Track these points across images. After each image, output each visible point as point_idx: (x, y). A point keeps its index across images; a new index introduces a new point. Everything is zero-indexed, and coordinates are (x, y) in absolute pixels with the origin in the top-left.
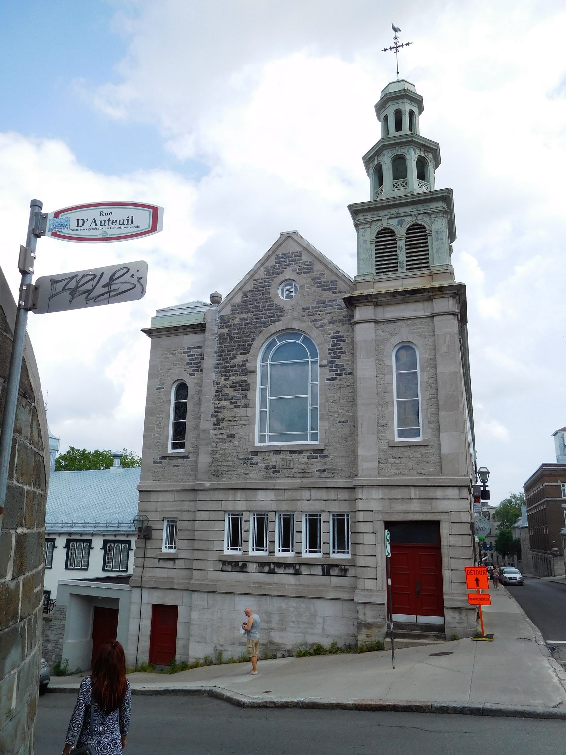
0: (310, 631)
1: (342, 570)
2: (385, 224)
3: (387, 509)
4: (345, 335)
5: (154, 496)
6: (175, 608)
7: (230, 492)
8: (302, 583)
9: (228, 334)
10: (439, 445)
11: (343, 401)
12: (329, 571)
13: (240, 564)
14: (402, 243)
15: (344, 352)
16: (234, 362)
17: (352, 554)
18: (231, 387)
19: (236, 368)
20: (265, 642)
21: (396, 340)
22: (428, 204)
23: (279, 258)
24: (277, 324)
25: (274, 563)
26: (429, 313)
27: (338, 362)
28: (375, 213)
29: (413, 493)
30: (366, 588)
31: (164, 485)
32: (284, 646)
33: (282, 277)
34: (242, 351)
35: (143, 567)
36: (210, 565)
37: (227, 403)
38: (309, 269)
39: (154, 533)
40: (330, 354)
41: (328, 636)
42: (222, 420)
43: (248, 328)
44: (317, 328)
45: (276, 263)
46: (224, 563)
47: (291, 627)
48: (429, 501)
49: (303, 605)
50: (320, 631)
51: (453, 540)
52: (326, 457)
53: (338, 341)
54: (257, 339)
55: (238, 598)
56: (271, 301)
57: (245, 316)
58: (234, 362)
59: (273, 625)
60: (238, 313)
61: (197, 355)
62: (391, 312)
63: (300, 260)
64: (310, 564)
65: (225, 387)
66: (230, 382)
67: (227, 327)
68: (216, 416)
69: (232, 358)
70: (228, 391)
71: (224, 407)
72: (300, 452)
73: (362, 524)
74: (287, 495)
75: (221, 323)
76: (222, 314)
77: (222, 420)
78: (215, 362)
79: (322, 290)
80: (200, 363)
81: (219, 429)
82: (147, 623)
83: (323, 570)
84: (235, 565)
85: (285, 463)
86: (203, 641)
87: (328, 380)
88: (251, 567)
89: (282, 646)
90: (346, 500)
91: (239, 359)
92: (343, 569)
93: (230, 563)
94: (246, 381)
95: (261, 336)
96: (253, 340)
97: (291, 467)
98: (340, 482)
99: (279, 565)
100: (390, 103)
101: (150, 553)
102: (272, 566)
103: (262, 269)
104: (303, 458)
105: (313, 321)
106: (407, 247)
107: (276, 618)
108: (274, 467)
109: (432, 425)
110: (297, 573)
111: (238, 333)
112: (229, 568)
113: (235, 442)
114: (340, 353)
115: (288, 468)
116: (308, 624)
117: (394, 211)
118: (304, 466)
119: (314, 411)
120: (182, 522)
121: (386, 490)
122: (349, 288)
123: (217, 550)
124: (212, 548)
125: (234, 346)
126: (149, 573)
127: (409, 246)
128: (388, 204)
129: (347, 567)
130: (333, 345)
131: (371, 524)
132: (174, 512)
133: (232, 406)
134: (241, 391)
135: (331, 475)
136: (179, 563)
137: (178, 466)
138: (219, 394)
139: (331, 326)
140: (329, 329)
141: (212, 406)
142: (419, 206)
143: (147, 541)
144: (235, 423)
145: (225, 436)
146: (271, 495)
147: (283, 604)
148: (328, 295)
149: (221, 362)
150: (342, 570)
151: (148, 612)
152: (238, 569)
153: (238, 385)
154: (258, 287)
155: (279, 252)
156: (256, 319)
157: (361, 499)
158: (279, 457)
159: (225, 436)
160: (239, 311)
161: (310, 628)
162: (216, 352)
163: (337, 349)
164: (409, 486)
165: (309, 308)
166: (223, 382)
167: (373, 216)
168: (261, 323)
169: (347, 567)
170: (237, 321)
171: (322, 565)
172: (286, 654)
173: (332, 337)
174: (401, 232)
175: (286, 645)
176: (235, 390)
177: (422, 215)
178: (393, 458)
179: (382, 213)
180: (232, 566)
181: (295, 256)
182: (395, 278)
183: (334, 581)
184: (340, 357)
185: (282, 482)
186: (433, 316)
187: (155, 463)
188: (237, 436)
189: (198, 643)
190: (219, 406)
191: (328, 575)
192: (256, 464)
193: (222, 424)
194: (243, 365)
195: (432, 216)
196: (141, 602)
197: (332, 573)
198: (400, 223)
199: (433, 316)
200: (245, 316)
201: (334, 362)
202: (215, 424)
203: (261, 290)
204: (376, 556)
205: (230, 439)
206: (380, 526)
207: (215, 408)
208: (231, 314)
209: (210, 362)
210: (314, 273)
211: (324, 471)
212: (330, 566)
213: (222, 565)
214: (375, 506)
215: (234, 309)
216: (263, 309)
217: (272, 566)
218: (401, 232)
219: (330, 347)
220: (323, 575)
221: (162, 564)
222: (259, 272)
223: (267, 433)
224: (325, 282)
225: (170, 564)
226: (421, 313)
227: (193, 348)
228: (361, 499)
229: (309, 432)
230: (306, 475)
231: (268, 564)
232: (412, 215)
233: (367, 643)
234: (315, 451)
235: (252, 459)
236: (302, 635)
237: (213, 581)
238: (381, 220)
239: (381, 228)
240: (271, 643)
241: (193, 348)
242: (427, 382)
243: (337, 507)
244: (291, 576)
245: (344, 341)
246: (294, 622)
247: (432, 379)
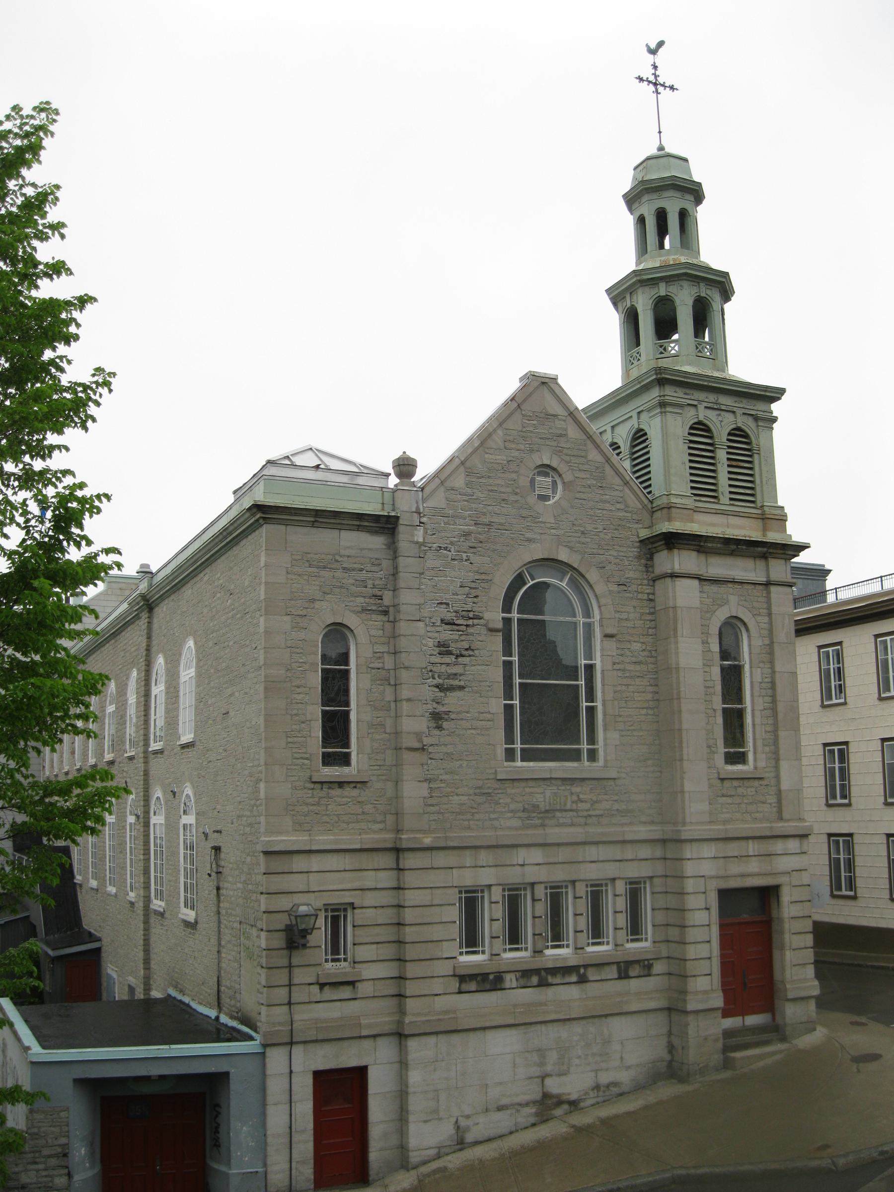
1: (644, 966)
2: (703, 414)
5: (299, 863)
6: (361, 1072)
7: (468, 852)
10: (778, 777)
11: (639, 699)
12: (626, 971)
13: (491, 977)
14: (722, 455)
17: (654, 942)
21: (722, 614)
22: (754, 402)
24: (533, 546)
26: (763, 579)
28: (688, 391)
29: (752, 847)
30: (699, 989)
31: (323, 840)
32: (568, 1097)
35: (290, 1004)
36: (437, 986)
41: (628, 1068)
46: (462, 979)
47: (576, 1065)
48: (767, 858)
49: (592, 1029)
55: (490, 1034)
59: (549, 1068)
62: (719, 567)
64: (600, 966)
73: (691, 897)
74: (563, 854)
82: (305, 1108)
85: (558, 800)
86: (434, 1115)
88: (510, 980)
89: (565, 1098)
90: (646, 859)
92: (646, 966)
93: (472, 977)
98: (643, 831)
99: (553, 971)
100: (670, 193)
101: (301, 976)
102: (543, 973)
106: (729, 463)
107: (552, 1056)
109: (767, 749)
110: (583, 980)
112: (473, 986)
115: (563, 808)
116: (601, 1055)
117: (712, 397)
119: (591, 711)
120: (364, 910)
121: (721, 845)
122: (641, 507)
123: (447, 958)
124: (439, 955)
126: (301, 1015)
127: (731, 461)
128: (710, 384)
129: (651, 962)
131: (703, 895)
132: (347, 893)
136: (365, 989)
142: (744, 401)
143: (294, 953)
146: (537, 856)
147: (562, 1032)
150: (644, 966)
151: (304, 1088)
152: (488, 987)
157: (689, 859)
161: (603, 1061)
164: (747, 838)
167: (688, 397)
169: (651, 962)
171: (618, 963)
174: (721, 435)
175: (569, 1094)
177: (746, 417)
178: (723, 796)
179: (701, 395)
180: (478, 982)
182: (718, 512)
183: (634, 984)
185: (555, 833)
186: (768, 584)
189: (425, 1122)
191: (627, 977)
195: (760, 424)
196: (291, 1072)
197: (631, 973)
199: (768, 584)
204: (709, 942)
206: (713, 900)
212: (629, 964)
213: (461, 982)
214: (708, 869)
217: (543, 973)
218: (721, 435)
220: (620, 978)
221: (328, 993)
222: (494, 437)
223: (518, 746)
225: (346, 992)
226: (752, 576)
228: (689, 859)
229: (585, 746)
231: (537, 971)
232: (734, 412)
233: (701, 1065)
236: (593, 1074)
237: (446, 1012)
238: (695, 406)
239: (696, 420)
240: (546, 1096)
242: (761, 683)
243: (634, 871)
244: (573, 986)
246: (579, 1057)
247: (766, 680)
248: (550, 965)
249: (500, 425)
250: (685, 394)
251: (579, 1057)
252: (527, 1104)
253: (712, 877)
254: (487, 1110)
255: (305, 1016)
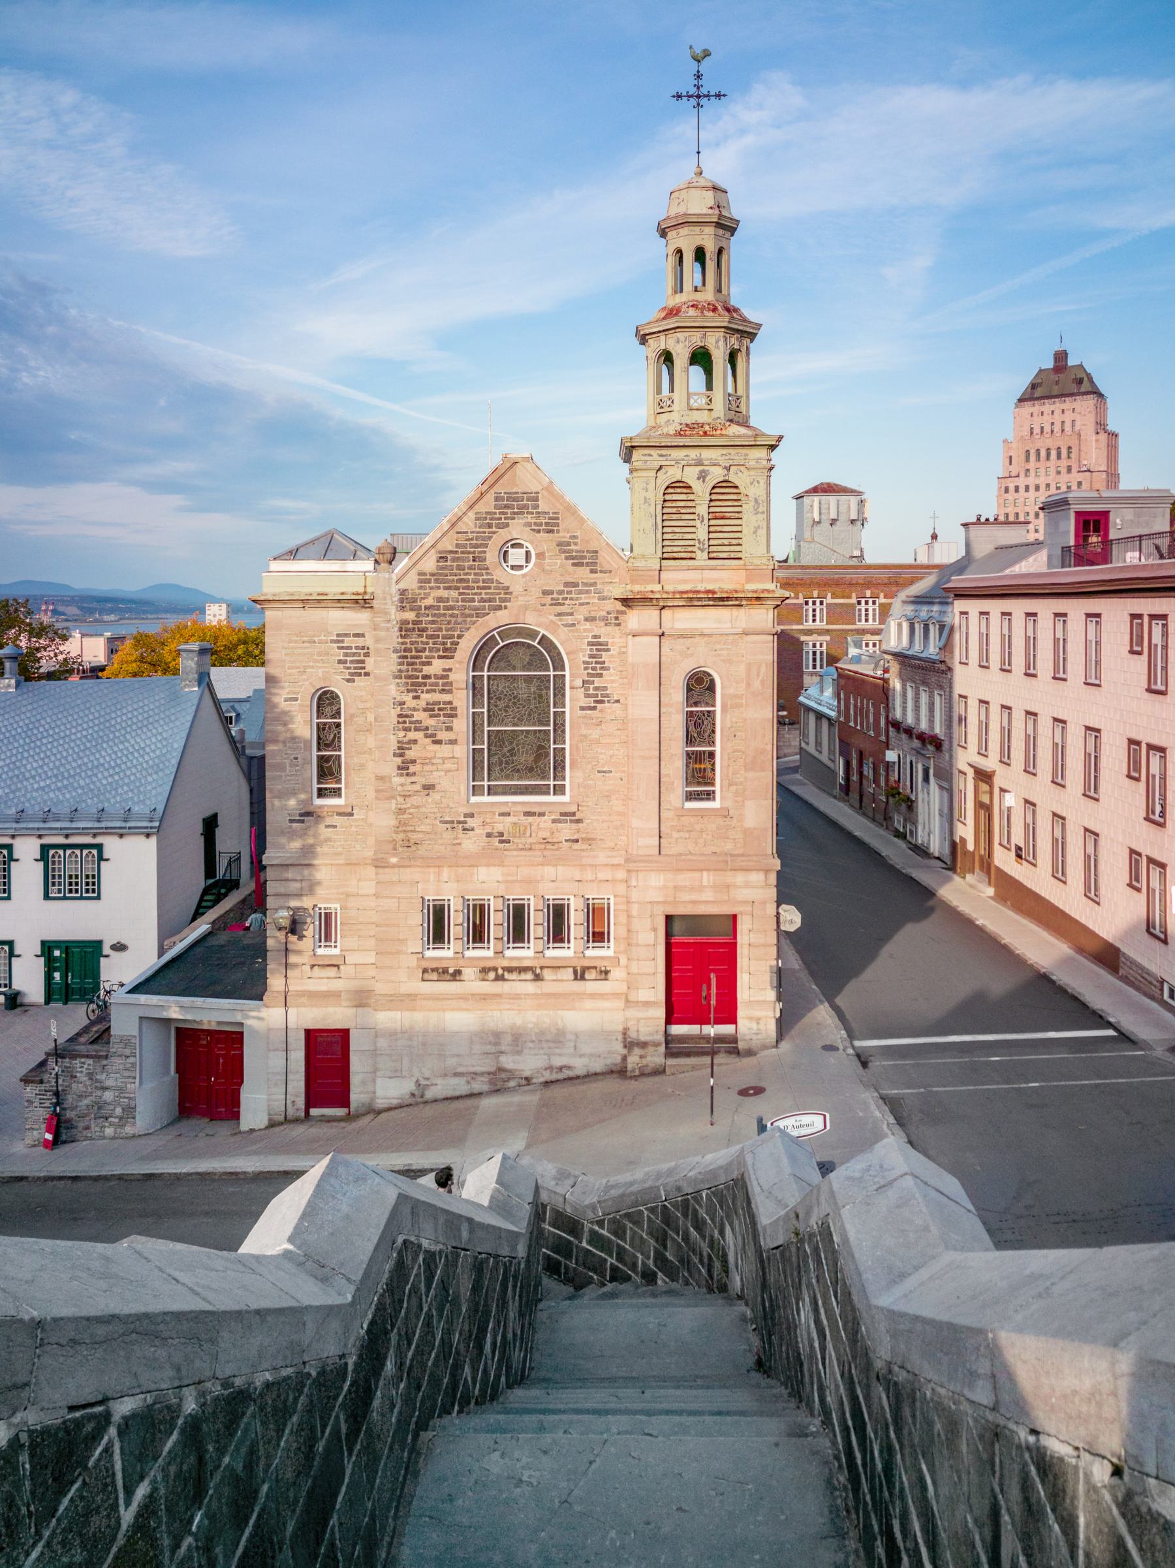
0: (558, 1051)
3: (671, 899)
4: (610, 641)
8: (545, 991)
9: (414, 623)
14: (702, 510)
15: (607, 669)
16: (427, 670)
18: (425, 710)
19: (433, 680)
20: (492, 1069)
21: (688, 666)
23: (502, 499)
24: (499, 613)
25: (504, 969)
27: (598, 682)
30: (640, 999)
33: (503, 535)
34: (441, 653)
37: (419, 735)
38: (551, 527)
39: (298, 926)
40: (586, 669)
42: (414, 762)
43: (451, 616)
44: (565, 626)
45: (496, 507)
46: (425, 971)
50: (572, 1050)
51: (754, 938)
52: (579, 821)
53: (598, 650)
54: (467, 634)
56: (487, 574)
57: (444, 594)
58: (427, 670)
59: (503, 1048)
60: (431, 588)
61: (357, 648)
63: (537, 507)
65: (414, 709)
66: (422, 703)
67: (412, 609)
68: (401, 755)
69: (423, 664)
70: (419, 716)
71: (415, 742)
72: (542, 814)
75: (402, 601)
76: (402, 586)
77: (414, 762)
78: (395, 668)
79: (574, 565)
80: (363, 662)
81: (407, 775)
83: (575, 972)
84: (443, 972)
87: (582, 708)
88: (469, 973)
91: (437, 666)
94: (450, 703)
95: (472, 630)
96: (460, 637)
97: (528, 834)
99: (510, 970)
102: (500, 972)
103: (471, 515)
104: (545, 822)
105: (559, 615)
108: (501, 834)
110: (538, 978)
111: (433, 622)
112: (435, 976)
113: (435, 796)
114: (602, 668)
118: (546, 834)
125: (427, 643)
130: (591, 656)
133: (429, 740)
134: (442, 718)
135: (585, 846)
137: (335, 827)
138: (404, 719)
139: (588, 625)
140: (585, 630)
141: (393, 740)
144: (434, 768)
145: (417, 787)
148: (583, 574)
149: (404, 667)
153: (436, 707)
154: (465, 546)
155: (500, 488)
156: (463, 601)
158: (509, 820)
159: (417, 787)
160: (432, 584)
162: (395, 651)
163: (596, 663)
164: (702, 870)
165: (552, 592)
166: (408, 698)
168: (471, 608)
170: (430, 601)
172: (524, 1082)
173: (590, 644)
176: (431, 716)
181: (528, 500)
184: (601, 675)
187: (291, 821)
188: (438, 787)
190: (405, 740)
191: (583, 978)
192: (473, 829)
193: (412, 769)
194: (443, 677)
197: (587, 976)
198: (702, 476)
200: (444, 594)
201: (593, 682)
202: (399, 768)
203: (469, 553)
205: (426, 792)
207: (399, 742)
208: (420, 588)
209: (384, 664)
210: (561, 534)
211: (577, 841)
212: (585, 969)
215: (423, 579)
216: (475, 585)
217: (500, 972)
218: (701, 491)
219: (587, 659)
220: (576, 979)
222: (465, 519)
224: (577, 551)
225: (332, 972)
227: (346, 635)
230: (549, 846)
231: (495, 969)
234: (563, 814)
235: (465, 822)
240: (501, 1070)
241: (346, 635)
244: (528, 983)
245: (608, 650)
246: (533, 1042)
248: (506, 964)
249: (471, 507)
250: (661, 456)
251: (533, 1042)
252: (482, 1074)
253: (658, 903)
254: (445, 1075)
255: (299, 988)
